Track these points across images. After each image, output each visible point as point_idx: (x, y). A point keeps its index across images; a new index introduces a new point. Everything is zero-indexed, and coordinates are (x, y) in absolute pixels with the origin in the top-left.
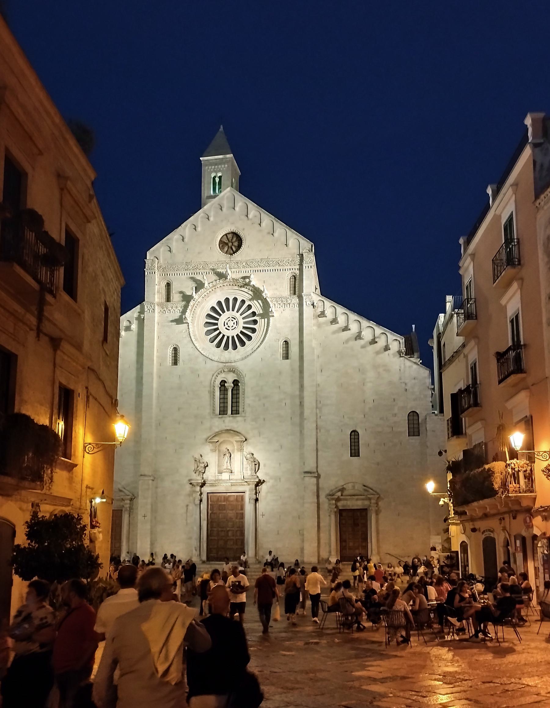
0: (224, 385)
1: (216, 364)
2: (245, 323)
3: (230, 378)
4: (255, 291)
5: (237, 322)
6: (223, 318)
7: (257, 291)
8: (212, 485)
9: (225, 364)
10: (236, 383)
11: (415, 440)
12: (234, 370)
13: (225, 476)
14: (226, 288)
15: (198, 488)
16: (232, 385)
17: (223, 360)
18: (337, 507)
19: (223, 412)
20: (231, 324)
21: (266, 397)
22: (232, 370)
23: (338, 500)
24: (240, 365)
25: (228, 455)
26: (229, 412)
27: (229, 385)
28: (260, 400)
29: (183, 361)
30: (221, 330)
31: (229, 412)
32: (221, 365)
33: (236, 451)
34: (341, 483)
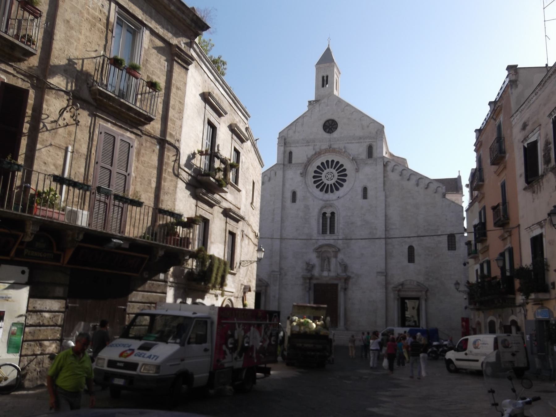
0: (325, 216)
1: (321, 202)
2: (339, 176)
3: (328, 211)
8: (317, 279)
9: (325, 202)
10: (333, 214)
11: (451, 253)
13: (325, 274)
15: (308, 281)
16: (330, 215)
17: (324, 198)
18: (399, 295)
19: (324, 232)
20: (330, 176)
21: (352, 223)
22: (331, 206)
23: (399, 291)
25: (327, 260)
26: (328, 232)
29: (299, 200)
30: (323, 180)
31: (328, 232)
32: (324, 202)
34: (402, 280)
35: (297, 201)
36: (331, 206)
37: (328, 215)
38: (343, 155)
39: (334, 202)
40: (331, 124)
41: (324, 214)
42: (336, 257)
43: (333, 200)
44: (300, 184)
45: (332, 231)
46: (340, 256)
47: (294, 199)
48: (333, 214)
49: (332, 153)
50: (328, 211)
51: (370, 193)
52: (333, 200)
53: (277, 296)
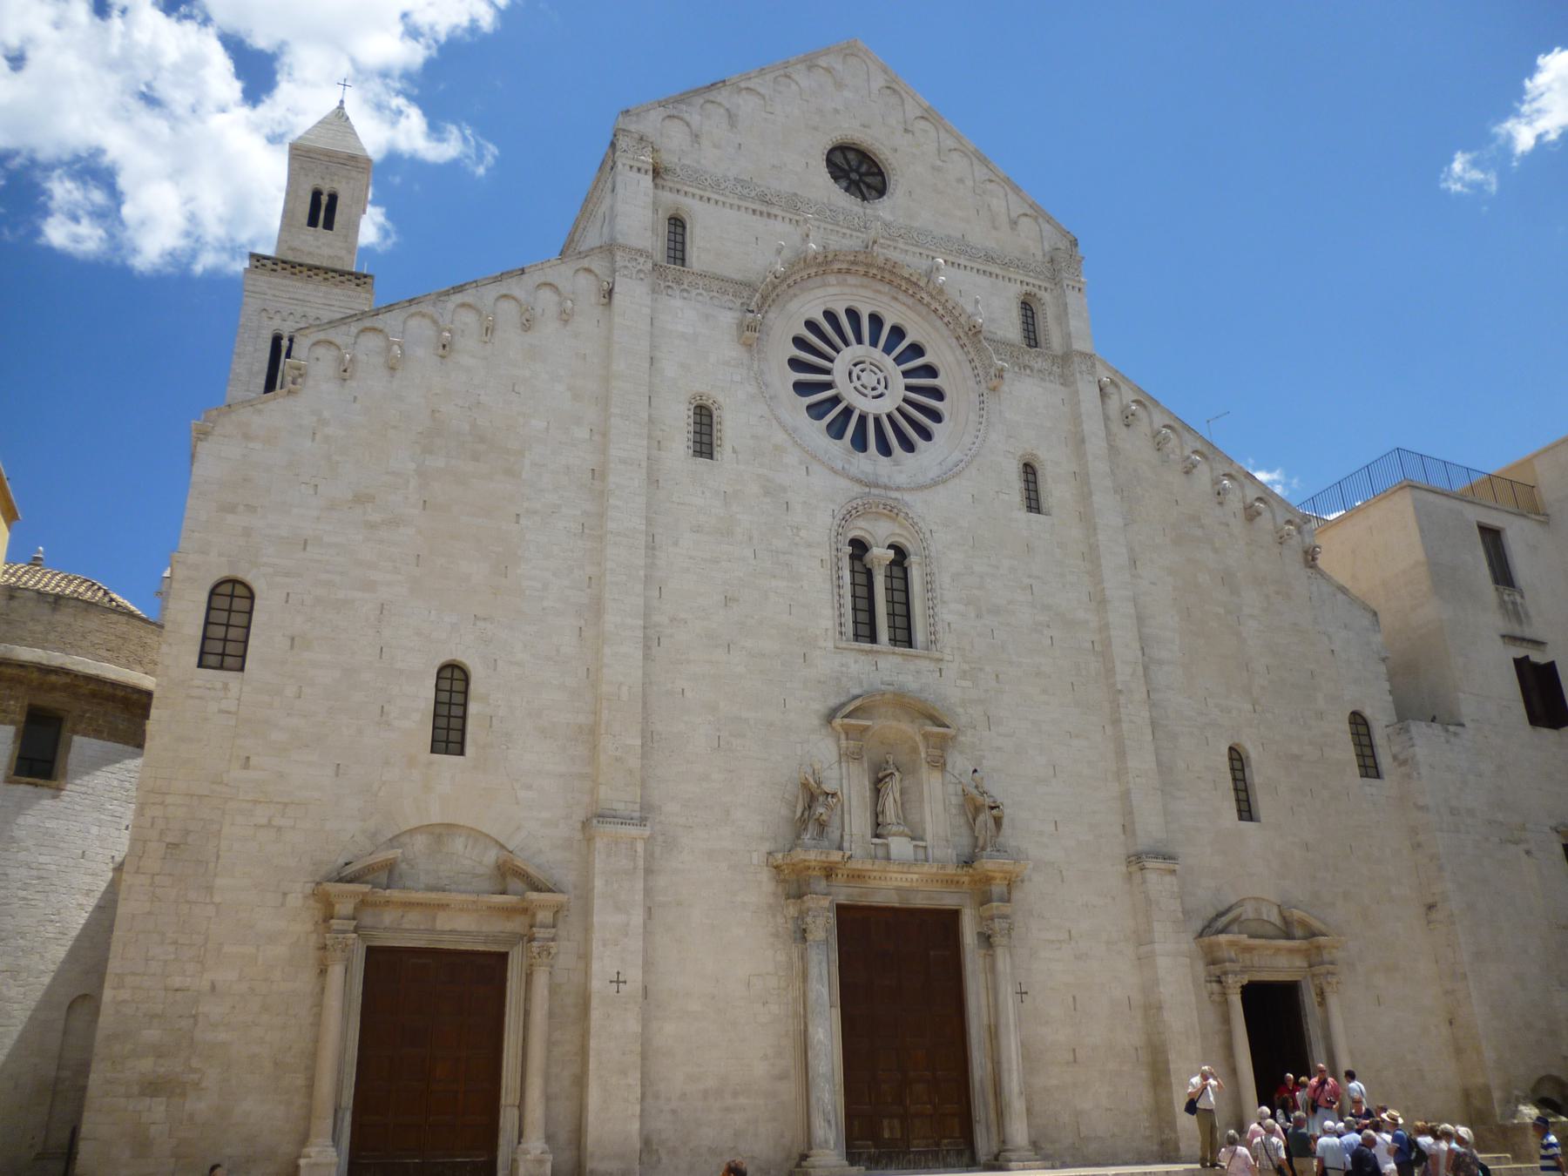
1: (843, 483)
4: (940, 308)
5: (885, 378)
6: (841, 364)
7: (945, 308)
9: (867, 490)
10: (901, 554)
12: (895, 511)
14: (851, 280)
22: (892, 511)
24: (916, 503)
27: (881, 555)
28: (979, 616)
29: (734, 451)
32: (857, 489)
33: (925, 766)
35: (724, 452)
36: (892, 511)
37: (881, 555)
38: (928, 305)
39: (907, 497)
40: (854, 167)
41: (859, 548)
42: (939, 764)
43: (898, 489)
44: (737, 378)
45: (904, 636)
46: (959, 762)
47: (704, 441)
48: (901, 554)
49: (879, 286)
50: (880, 535)
51: (1054, 490)
52: (898, 489)
53: (634, 976)
